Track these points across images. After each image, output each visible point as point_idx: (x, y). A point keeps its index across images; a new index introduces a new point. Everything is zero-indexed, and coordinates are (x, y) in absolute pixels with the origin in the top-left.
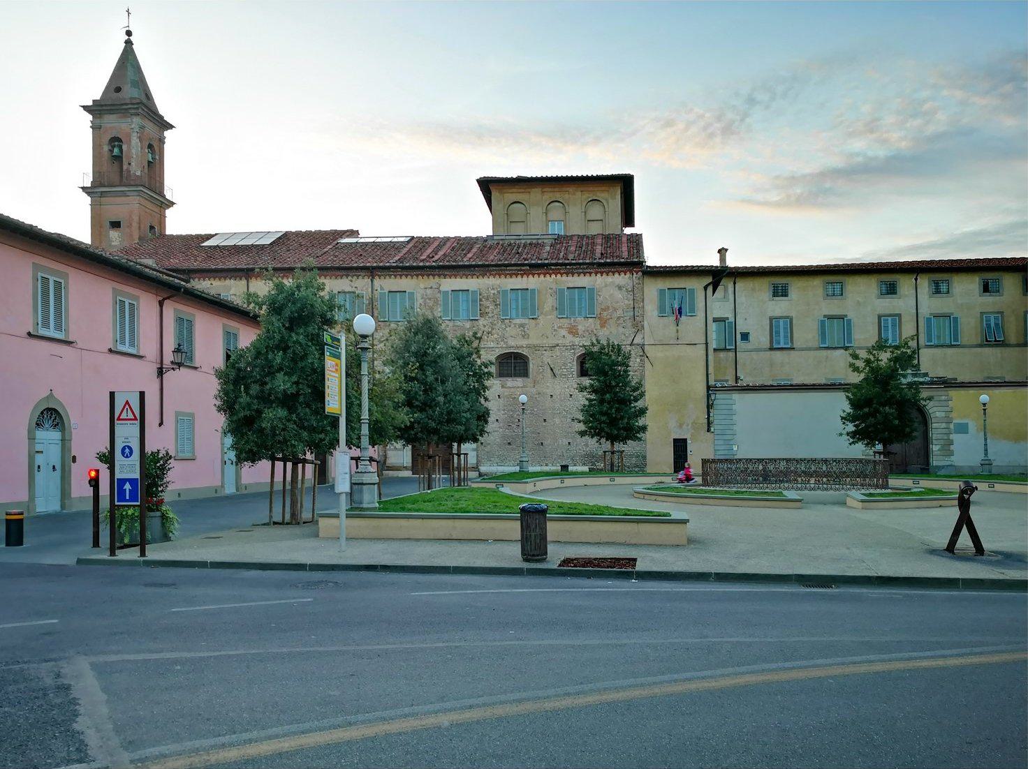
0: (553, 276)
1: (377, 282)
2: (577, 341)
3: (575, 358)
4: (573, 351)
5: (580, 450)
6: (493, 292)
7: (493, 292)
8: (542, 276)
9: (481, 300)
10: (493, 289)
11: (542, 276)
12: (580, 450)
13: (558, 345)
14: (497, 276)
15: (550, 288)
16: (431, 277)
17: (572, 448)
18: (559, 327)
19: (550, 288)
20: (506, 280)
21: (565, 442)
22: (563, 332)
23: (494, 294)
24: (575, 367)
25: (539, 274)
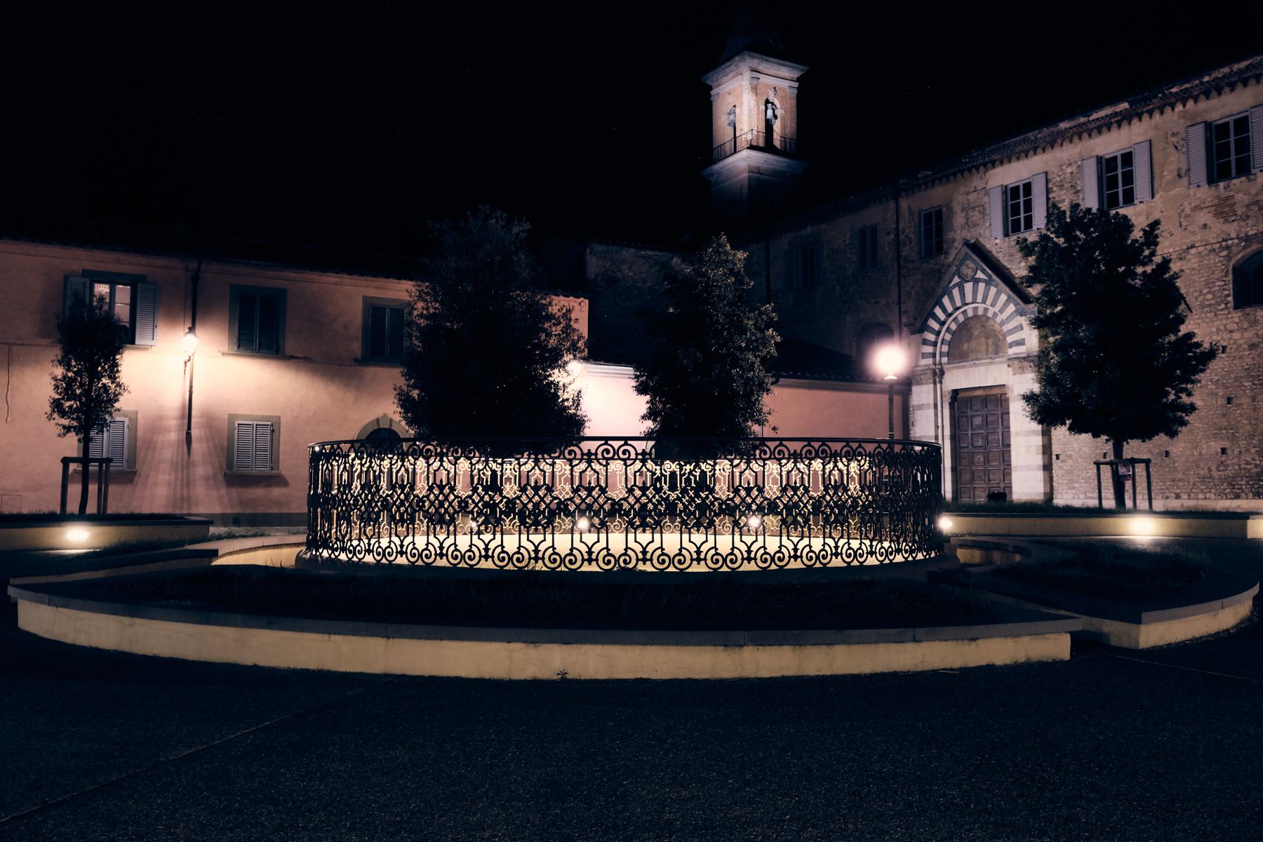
0: (1179, 107)
1: (904, 203)
2: (1232, 229)
3: (1231, 267)
4: (1225, 253)
5: (1248, 463)
6: (1069, 170)
7: (1069, 170)
8: (1157, 116)
9: (1048, 191)
10: (1070, 165)
11: (1157, 116)
12: (1248, 463)
13: (1193, 246)
14: (1076, 139)
15: (1174, 135)
16: (959, 175)
17: (1231, 460)
18: (1194, 209)
19: (1174, 135)
20: (1092, 141)
21: (1216, 446)
22: (1204, 217)
23: (1072, 173)
24: (1231, 286)
25: (1151, 113)
